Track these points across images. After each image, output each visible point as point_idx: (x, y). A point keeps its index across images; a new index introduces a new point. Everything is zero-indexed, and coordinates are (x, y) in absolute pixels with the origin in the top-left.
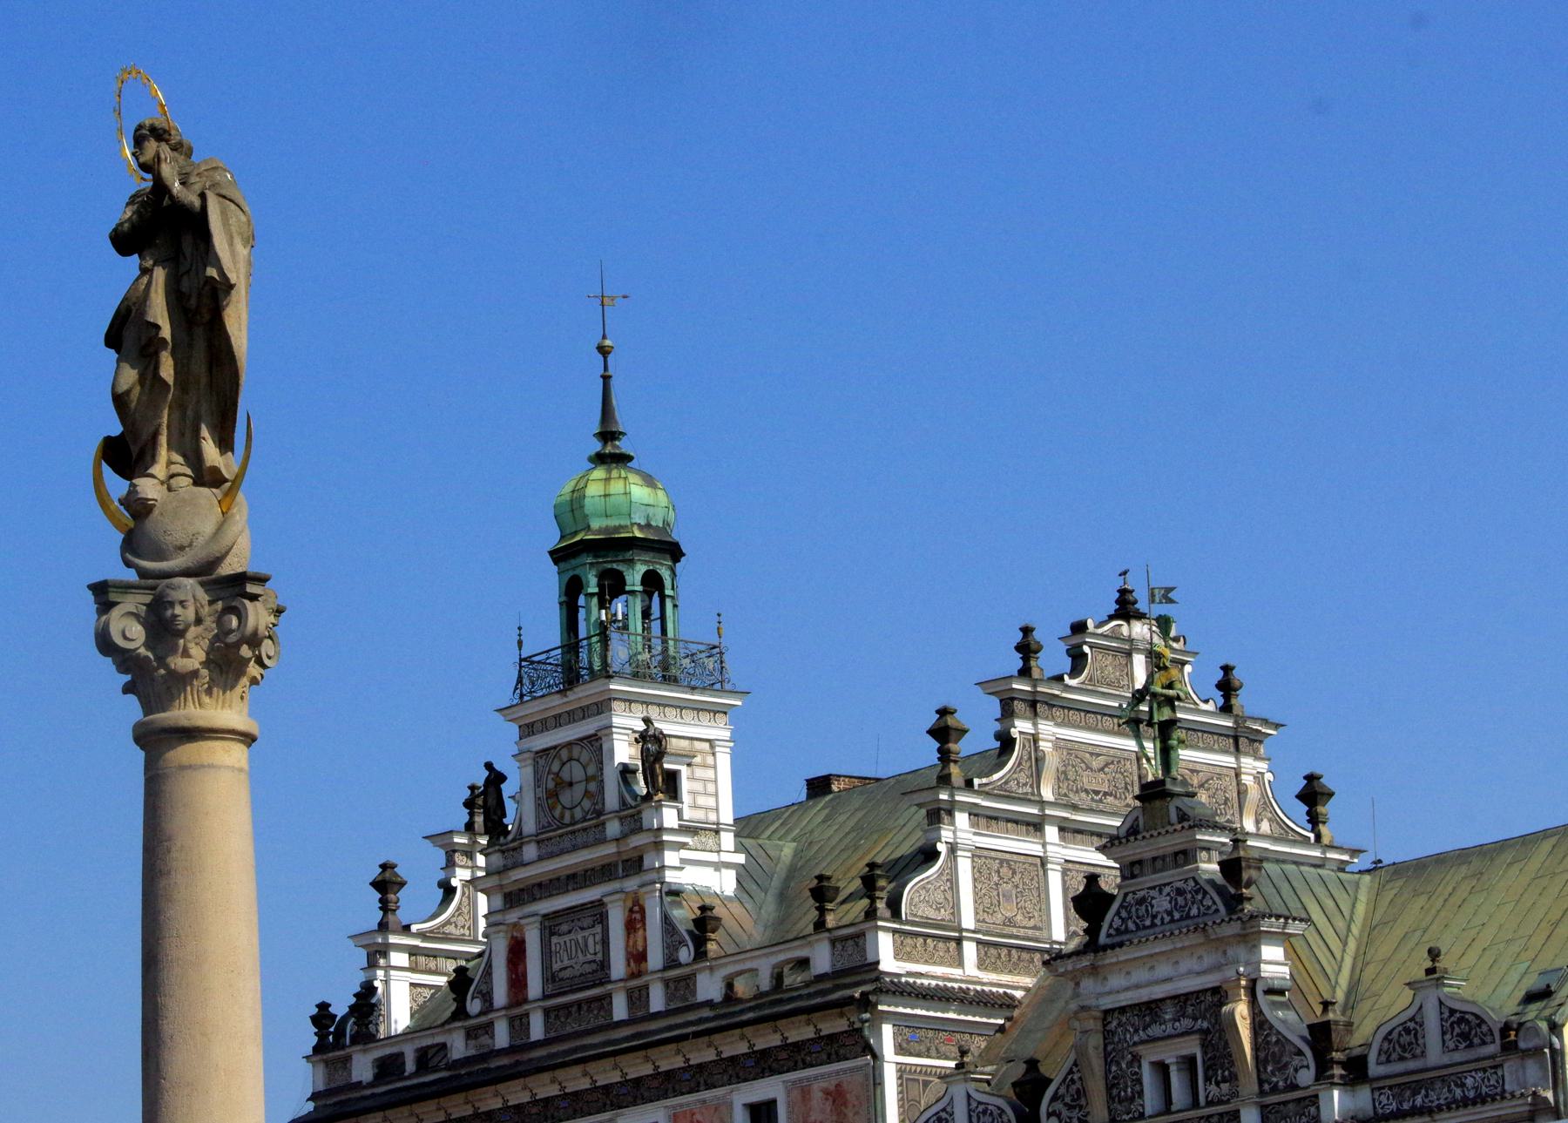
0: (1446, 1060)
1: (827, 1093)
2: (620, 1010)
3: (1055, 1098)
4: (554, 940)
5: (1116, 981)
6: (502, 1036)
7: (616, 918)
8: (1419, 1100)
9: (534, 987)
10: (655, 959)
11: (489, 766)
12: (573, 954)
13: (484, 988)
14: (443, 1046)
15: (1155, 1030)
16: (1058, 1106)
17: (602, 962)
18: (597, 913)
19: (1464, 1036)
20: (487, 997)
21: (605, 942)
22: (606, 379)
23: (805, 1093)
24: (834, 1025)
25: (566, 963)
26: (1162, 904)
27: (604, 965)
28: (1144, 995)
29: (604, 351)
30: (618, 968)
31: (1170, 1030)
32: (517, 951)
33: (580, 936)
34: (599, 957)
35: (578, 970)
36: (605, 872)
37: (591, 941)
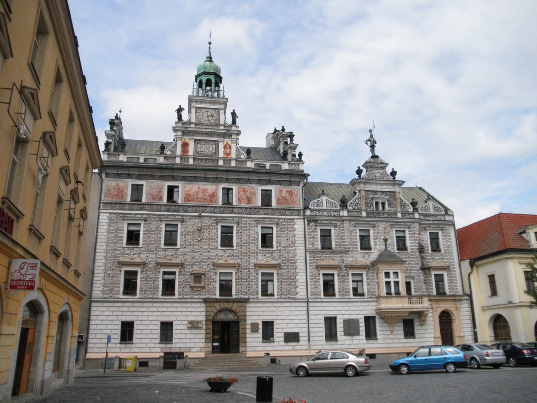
0: (434, 213)
1: (287, 191)
2: (221, 163)
3: (351, 203)
4: (198, 145)
5: (368, 186)
6: (178, 161)
7: (221, 146)
8: (428, 218)
9: (191, 152)
10: (233, 155)
11: (180, 106)
12: (207, 149)
13: (172, 150)
14: (156, 159)
15: (376, 196)
16: (352, 205)
17: (215, 153)
18: (216, 143)
19: (437, 210)
20: (174, 152)
21: (217, 149)
22: (210, 48)
23: (281, 191)
24: (297, 179)
25: (202, 150)
26: (378, 175)
27: (216, 153)
28: (375, 190)
29: (210, 43)
30: (221, 154)
31: (379, 196)
32: (185, 145)
33: (208, 146)
34: (214, 151)
35: (206, 152)
36: (219, 135)
37: (211, 148)
